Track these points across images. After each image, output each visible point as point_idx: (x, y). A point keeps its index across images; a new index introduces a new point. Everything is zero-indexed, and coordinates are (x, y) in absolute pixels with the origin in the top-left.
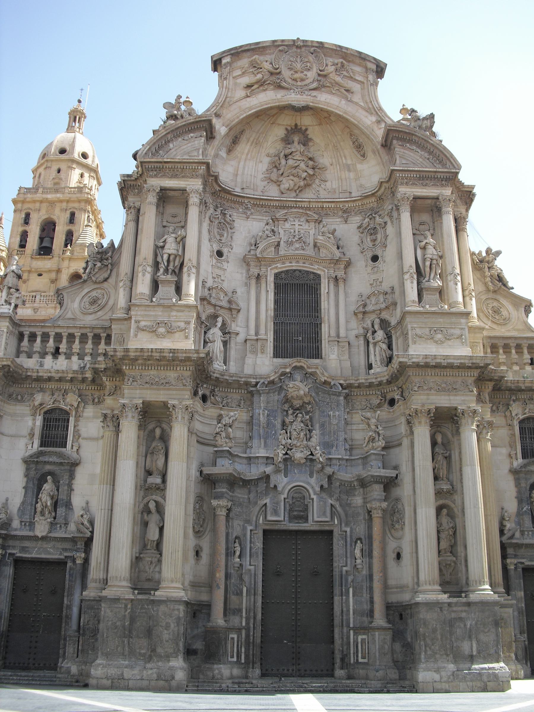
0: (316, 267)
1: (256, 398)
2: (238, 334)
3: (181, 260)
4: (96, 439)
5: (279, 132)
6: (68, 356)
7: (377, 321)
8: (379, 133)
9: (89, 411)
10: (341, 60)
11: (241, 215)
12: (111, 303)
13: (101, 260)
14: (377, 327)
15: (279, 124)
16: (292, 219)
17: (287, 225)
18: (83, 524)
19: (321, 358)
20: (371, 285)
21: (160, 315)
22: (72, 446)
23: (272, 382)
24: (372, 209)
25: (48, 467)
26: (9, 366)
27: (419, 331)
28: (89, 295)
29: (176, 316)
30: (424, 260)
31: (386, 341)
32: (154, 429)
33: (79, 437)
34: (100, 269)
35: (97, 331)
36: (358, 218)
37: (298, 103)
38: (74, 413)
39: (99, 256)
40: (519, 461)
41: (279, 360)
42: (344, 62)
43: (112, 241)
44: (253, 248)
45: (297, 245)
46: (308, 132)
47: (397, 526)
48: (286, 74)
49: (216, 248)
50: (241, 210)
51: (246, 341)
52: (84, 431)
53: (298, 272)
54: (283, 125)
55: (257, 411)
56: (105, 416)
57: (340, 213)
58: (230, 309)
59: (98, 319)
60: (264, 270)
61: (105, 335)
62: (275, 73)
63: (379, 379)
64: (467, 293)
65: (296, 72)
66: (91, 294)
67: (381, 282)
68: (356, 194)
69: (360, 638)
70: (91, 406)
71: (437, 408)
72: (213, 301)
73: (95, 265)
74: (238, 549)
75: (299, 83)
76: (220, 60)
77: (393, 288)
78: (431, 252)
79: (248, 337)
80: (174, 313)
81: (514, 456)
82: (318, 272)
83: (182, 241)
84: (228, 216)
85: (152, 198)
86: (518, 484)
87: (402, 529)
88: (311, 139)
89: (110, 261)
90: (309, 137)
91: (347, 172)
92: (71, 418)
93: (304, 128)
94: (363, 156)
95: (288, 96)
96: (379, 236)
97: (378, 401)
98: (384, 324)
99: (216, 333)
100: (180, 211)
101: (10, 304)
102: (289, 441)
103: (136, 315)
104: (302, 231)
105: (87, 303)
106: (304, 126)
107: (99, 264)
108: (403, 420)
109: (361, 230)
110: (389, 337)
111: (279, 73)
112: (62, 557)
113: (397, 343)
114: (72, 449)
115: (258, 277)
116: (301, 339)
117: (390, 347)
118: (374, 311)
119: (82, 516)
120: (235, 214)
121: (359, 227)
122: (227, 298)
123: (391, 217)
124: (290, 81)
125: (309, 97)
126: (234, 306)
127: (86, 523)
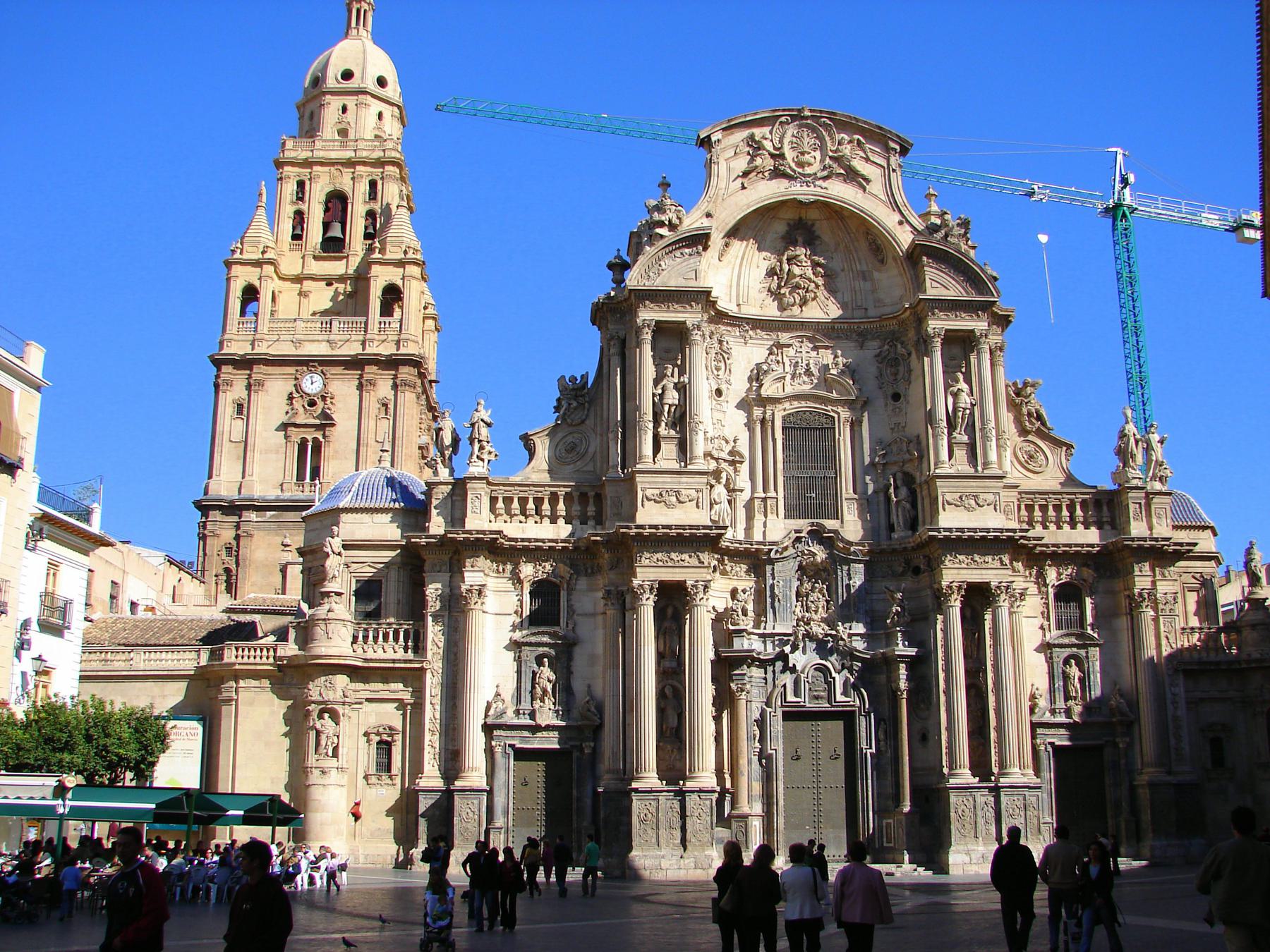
0: (829, 408)
1: (768, 568)
2: (742, 491)
3: (683, 409)
4: (594, 615)
5: (780, 228)
6: (554, 520)
7: (899, 475)
8: (905, 238)
9: (582, 583)
10: (856, 137)
11: (738, 340)
12: (591, 450)
13: (576, 397)
14: (899, 482)
15: (779, 218)
16: (798, 345)
17: (791, 352)
18: (589, 710)
19: (838, 519)
20: (892, 429)
21: (669, 482)
22: (567, 623)
23: (786, 548)
24: (893, 332)
25: (542, 650)
26: (497, 539)
27: (948, 497)
28: (564, 441)
29: (687, 483)
30: (955, 409)
31: (910, 499)
32: (667, 606)
33: (574, 613)
34: (575, 409)
35: (585, 489)
36: (875, 343)
37: (806, 197)
38: (565, 586)
39: (574, 393)
40: (1053, 635)
41: (792, 521)
42: (861, 138)
43: (587, 373)
44: (754, 384)
45: (806, 378)
46: (814, 228)
47: (922, 706)
48: (790, 155)
49: (715, 387)
50: (738, 334)
51: (752, 499)
52: (577, 606)
53: (808, 413)
54: (784, 219)
55: (769, 581)
56: (608, 592)
57: (854, 335)
58: (732, 463)
59: (578, 470)
60: (769, 413)
61: (593, 493)
62: (778, 156)
63: (903, 546)
64: (1001, 442)
65: (803, 154)
66: (567, 438)
67: (904, 427)
68: (871, 312)
69: (885, 821)
70: (585, 578)
71: (969, 584)
72: (715, 454)
73: (570, 404)
74: (757, 732)
75: (808, 170)
76: (709, 137)
77: (918, 436)
78: (965, 400)
79: (756, 495)
80: (684, 480)
81: (1046, 627)
82: (832, 414)
83: (682, 389)
84: (725, 343)
85: (647, 336)
86: (1050, 661)
87: (928, 709)
88: (819, 237)
89: (587, 399)
90: (817, 233)
91: (862, 283)
92: (562, 592)
93: (810, 223)
94: (882, 262)
95: (793, 188)
96: (901, 369)
97: (901, 569)
98: (909, 480)
99: (720, 491)
100: (675, 345)
101: (483, 460)
102: (807, 615)
103: (642, 482)
104: (811, 361)
105: (563, 451)
106: (810, 220)
107: (575, 404)
108: (929, 592)
109: (879, 359)
110: (913, 494)
111: (782, 156)
112: (567, 746)
113: (923, 504)
114: (567, 626)
115: (763, 421)
116: (814, 495)
117: (914, 505)
118: (895, 463)
119: (588, 702)
120: (732, 339)
121: (876, 356)
122: (728, 448)
123: (917, 351)
124: (793, 165)
125: (818, 189)
126: (737, 458)
127: (593, 709)
